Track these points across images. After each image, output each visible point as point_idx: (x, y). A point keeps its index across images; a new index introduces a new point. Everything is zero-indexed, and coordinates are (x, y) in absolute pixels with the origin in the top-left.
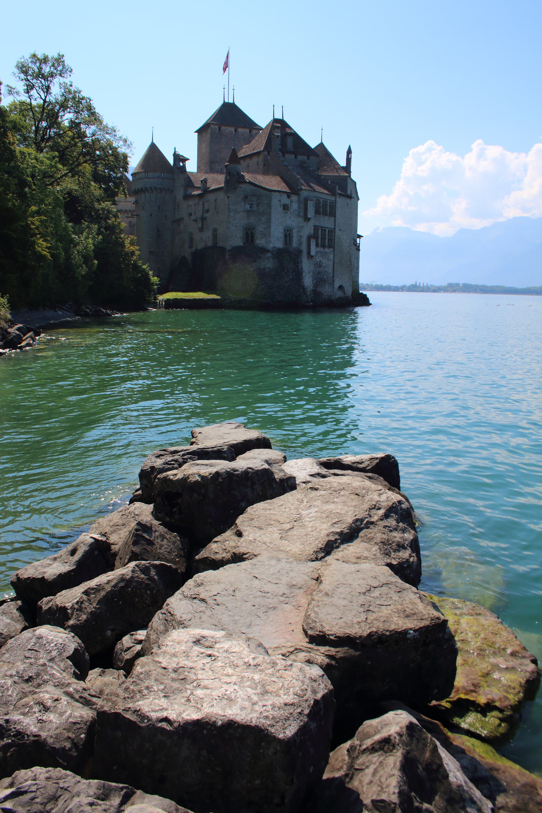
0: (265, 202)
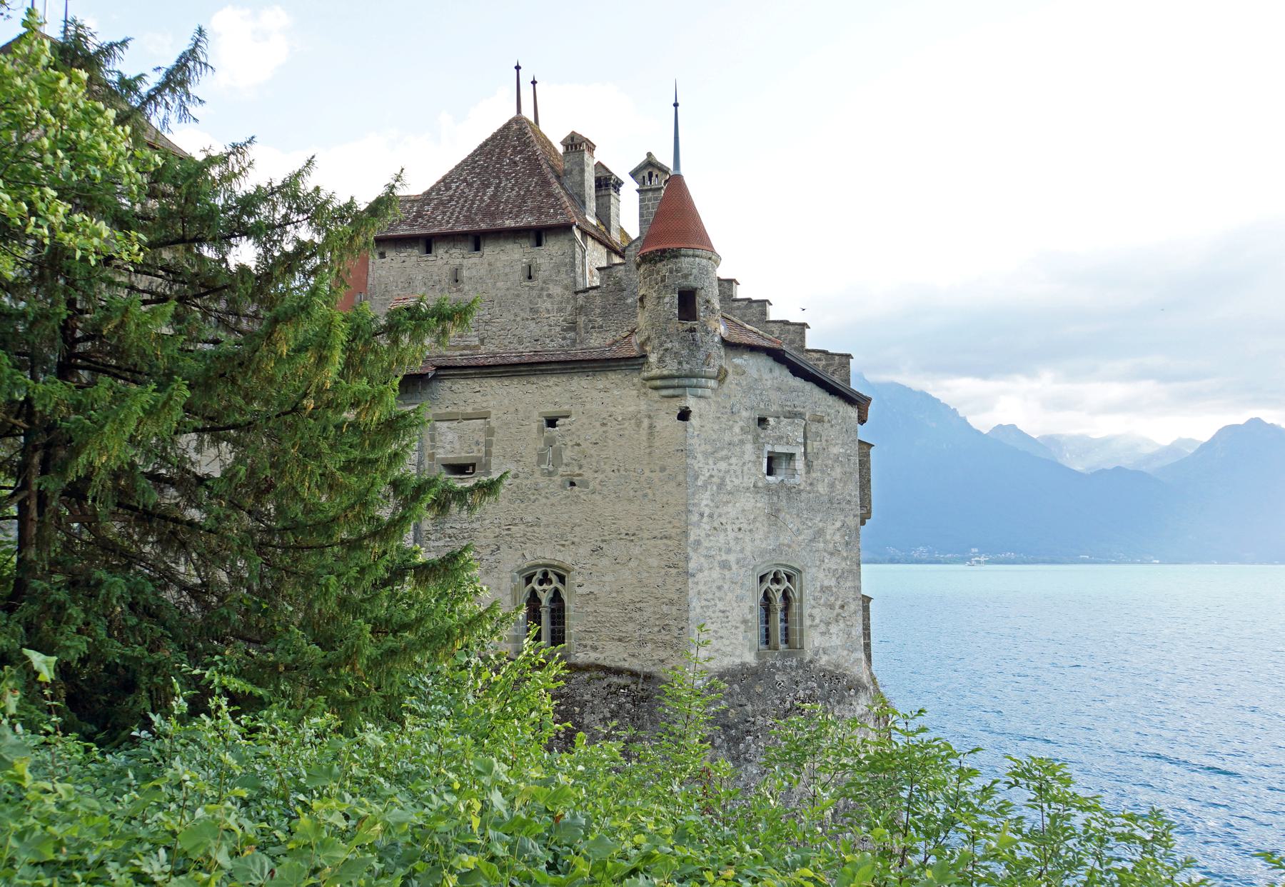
0: (836, 450)
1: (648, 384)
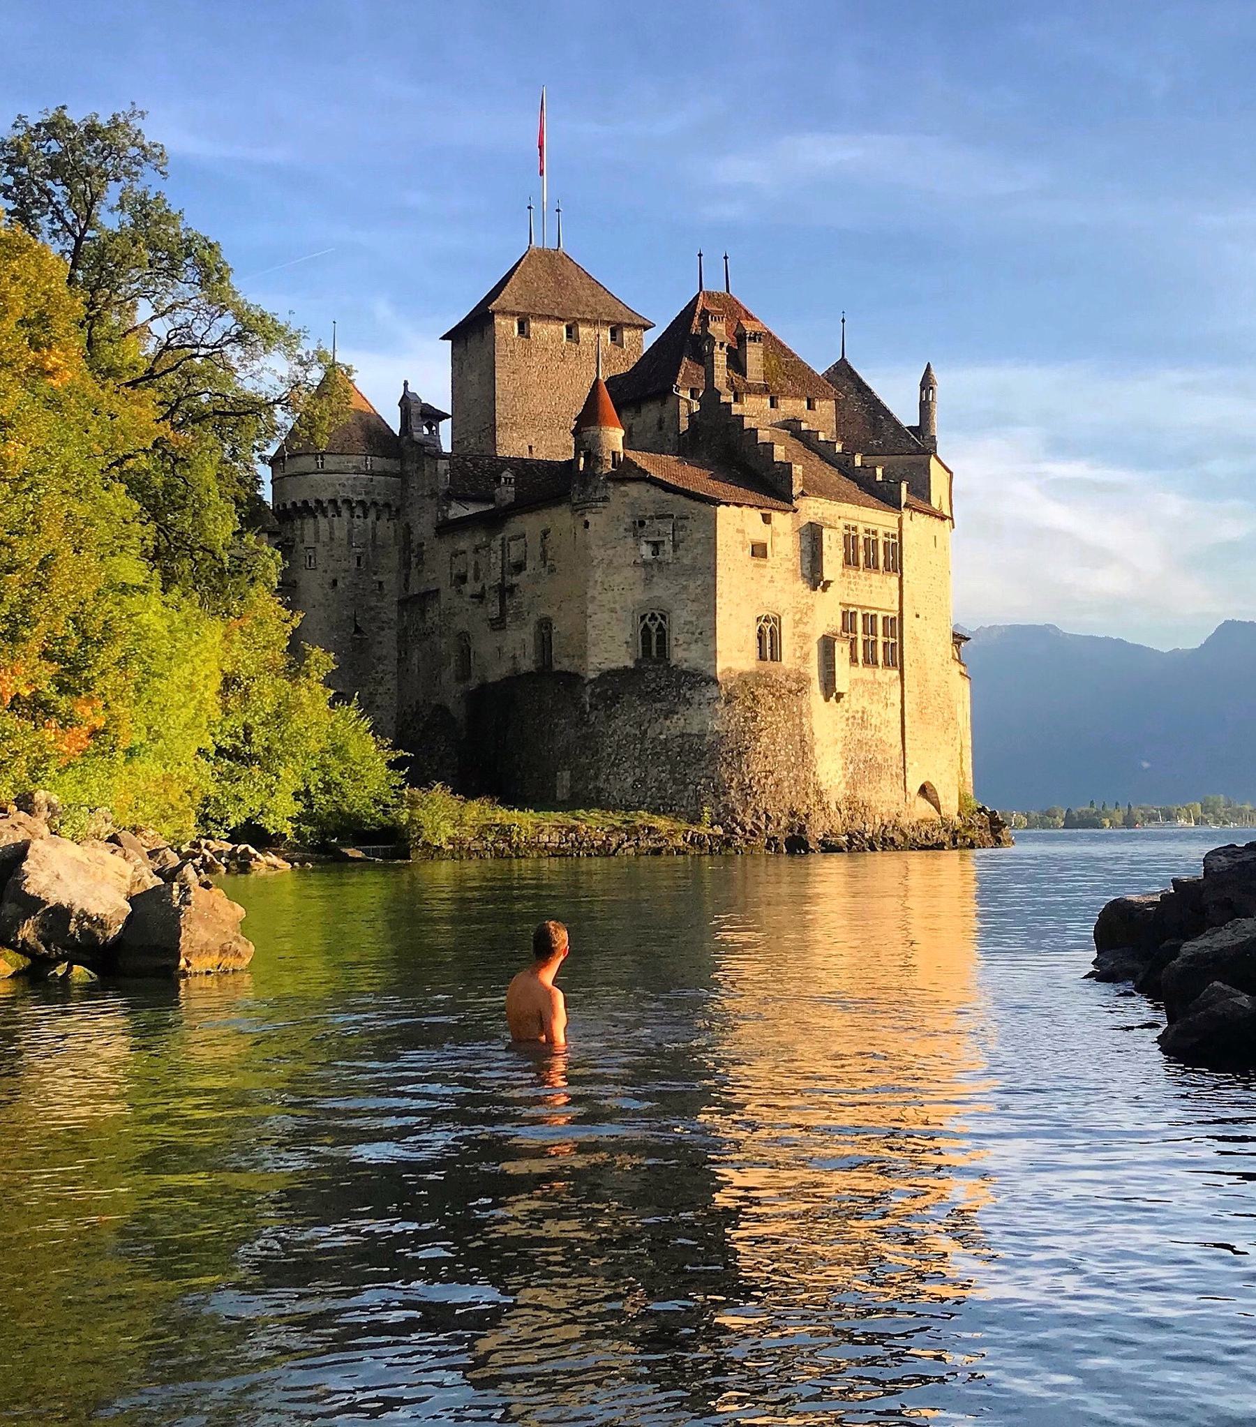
0: (698, 536)
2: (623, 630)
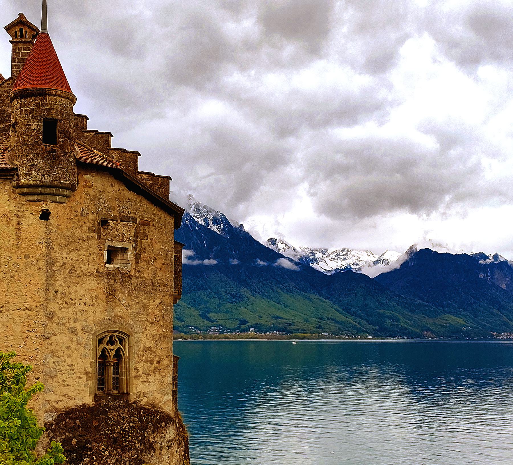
1: (18, 190)
2: (83, 357)
